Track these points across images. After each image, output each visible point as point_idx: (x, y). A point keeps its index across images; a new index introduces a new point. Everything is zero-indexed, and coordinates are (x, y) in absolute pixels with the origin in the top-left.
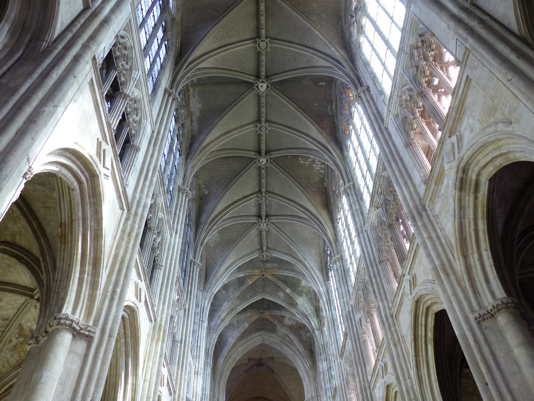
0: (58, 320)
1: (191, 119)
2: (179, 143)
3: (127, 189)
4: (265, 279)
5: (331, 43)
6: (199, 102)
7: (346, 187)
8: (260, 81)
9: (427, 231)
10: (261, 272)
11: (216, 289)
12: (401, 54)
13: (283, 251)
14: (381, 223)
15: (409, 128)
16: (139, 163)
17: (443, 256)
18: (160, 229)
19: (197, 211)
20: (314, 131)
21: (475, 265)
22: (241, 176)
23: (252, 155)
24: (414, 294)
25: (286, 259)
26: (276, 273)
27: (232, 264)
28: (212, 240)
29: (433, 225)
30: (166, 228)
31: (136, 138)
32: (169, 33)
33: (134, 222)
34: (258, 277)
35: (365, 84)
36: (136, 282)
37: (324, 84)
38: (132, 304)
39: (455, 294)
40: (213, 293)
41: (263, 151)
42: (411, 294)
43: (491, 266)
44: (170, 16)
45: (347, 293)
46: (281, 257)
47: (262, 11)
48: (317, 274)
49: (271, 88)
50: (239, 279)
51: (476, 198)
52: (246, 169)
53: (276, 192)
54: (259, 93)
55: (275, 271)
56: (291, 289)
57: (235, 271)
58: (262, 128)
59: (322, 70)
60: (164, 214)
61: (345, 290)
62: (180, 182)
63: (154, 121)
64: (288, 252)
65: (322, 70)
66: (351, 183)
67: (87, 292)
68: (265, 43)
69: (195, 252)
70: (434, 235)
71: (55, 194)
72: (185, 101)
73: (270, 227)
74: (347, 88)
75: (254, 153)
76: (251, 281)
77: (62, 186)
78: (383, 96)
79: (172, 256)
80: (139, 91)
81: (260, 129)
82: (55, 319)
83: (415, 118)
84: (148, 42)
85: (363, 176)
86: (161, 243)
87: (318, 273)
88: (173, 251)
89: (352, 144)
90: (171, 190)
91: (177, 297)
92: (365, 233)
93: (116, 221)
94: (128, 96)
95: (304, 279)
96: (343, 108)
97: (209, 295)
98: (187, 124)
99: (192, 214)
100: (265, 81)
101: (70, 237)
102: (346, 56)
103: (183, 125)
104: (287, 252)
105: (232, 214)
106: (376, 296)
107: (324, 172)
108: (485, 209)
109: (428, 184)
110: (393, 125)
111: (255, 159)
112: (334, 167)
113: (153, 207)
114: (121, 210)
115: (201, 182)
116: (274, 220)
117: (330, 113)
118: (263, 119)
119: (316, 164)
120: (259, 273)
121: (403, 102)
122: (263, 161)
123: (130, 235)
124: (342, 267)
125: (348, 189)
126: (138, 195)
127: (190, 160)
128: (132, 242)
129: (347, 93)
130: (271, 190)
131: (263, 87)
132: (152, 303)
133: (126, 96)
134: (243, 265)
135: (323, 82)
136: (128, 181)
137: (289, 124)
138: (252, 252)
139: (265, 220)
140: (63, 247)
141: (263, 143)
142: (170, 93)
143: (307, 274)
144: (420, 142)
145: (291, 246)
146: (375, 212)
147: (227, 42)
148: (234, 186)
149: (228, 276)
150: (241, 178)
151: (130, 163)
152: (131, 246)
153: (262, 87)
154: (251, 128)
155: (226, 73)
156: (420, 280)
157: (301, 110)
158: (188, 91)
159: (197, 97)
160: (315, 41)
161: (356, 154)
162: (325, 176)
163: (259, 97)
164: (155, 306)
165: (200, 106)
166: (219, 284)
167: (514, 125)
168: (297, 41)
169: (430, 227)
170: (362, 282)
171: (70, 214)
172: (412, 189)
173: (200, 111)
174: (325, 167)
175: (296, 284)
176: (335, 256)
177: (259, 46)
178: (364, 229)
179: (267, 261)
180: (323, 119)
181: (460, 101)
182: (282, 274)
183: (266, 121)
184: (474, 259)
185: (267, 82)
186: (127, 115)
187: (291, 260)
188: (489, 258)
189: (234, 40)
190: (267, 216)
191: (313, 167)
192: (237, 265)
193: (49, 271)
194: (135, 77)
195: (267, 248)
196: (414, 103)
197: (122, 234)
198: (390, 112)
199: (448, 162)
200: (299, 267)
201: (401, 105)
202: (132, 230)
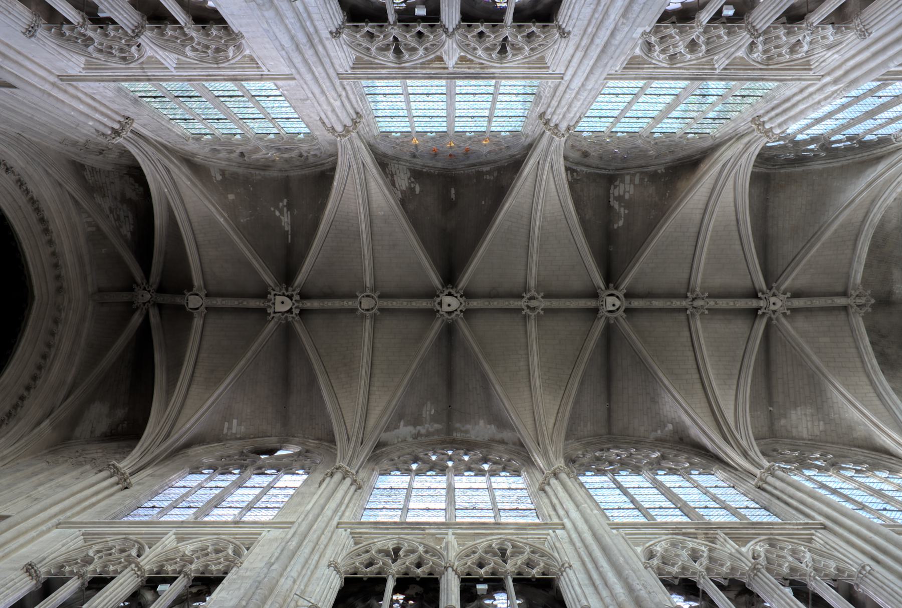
37: (453, 191)
53: (686, 276)
54: (461, 311)
68: (362, 301)
73: (783, 288)
81: (533, 309)
100: (438, 300)
107: (638, 175)
111: (607, 319)
117: (496, 174)
119: (625, 192)
135: (449, 192)
153: (449, 305)
159: (469, 427)
165: (482, 422)
174: (628, 174)
185: (441, 295)
195: (845, 294)
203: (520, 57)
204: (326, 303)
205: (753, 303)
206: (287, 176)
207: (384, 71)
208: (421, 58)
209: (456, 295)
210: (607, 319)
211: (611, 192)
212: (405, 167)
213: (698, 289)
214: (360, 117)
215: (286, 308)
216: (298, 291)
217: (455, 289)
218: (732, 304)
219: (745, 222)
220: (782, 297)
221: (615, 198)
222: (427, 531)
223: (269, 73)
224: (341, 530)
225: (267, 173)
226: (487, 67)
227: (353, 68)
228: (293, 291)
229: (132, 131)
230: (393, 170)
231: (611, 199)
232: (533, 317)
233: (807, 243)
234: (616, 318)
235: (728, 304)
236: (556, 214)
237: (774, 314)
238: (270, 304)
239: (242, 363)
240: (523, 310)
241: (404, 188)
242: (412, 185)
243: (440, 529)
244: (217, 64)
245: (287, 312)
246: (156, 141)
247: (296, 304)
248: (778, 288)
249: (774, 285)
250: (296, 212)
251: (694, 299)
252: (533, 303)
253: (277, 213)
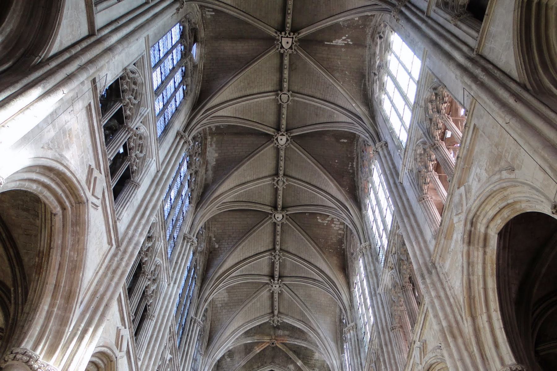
0: (14, 355)
1: (206, 167)
2: (189, 190)
3: (118, 224)
4: (275, 348)
5: (352, 99)
6: (215, 151)
7: (361, 247)
8: (280, 134)
9: (436, 290)
11: (219, 355)
12: (417, 107)
14: (395, 286)
15: (423, 182)
16: (137, 199)
17: (451, 317)
18: (156, 276)
19: (204, 265)
20: (333, 188)
21: (484, 327)
22: (254, 231)
23: (268, 209)
24: (424, 364)
25: (298, 327)
26: (287, 342)
27: (239, 327)
28: (220, 299)
29: (442, 284)
30: (164, 276)
31: (138, 175)
32: (189, 79)
33: (122, 259)
34: (268, 345)
35: (383, 140)
36: (118, 328)
37: (345, 141)
38: (109, 352)
39: (462, 359)
40: (215, 359)
41: (279, 206)
42: (421, 364)
43: (501, 328)
44: (192, 63)
45: (360, 366)
46: (293, 324)
47: (286, 65)
48: (331, 345)
49: (291, 141)
50: (246, 345)
51: (485, 253)
52: (260, 224)
53: (291, 251)
54: (278, 146)
55: (286, 339)
56: (302, 361)
57: (241, 335)
58: (279, 182)
59: (342, 125)
60: (163, 260)
61: (358, 363)
62: (186, 229)
63: (161, 162)
64: (301, 319)
65: (342, 125)
66: (367, 243)
67: (54, 328)
69: (198, 308)
70: (442, 294)
71: (38, 222)
72: (201, 149)
73: (283, 289)
74: (368, 145)
75: (270, 208)
76: (259, 349)
77: (45, 212)
78: (399, 151)
79: (167, 307)
80: (146, 129)
81: (277, 182)
82: (12, 353)
83: (428, 171)
84: (162, 82)
85: (379, 234)
86: (156, 292)
87: (333, 344)
88: (169, 302)
89: (371, 201)
90: (176, 237)
91: (170, 356)
92: (378, 296)
93: (101, 256)
94: (132, 130)
95: (317, 350)
96: (363, 166)
97: (210, 360)
98: (201, 173)
99: (198, 268)
100: (285, 134)
101: (45, 266)
102: (367, 112)
103: (196, 172)
104: (300, 319)
105: (242, 271)
106: (386, 367)
107: (343, 233)
108: (495, 266)
109: (438, 238)
110: (408, 180)
111: (271, 214)
112: (351, 226)
113: (150, 251)
114: (109, 245)
115: (212, 235)
116: (287, 281)
117: (351, 171)
118: (281, 173)
119: (335, 224)
120: (268, 341)
121: (418, 156)
122: (279, 216)
123: (114, 272)
124: (356, 336)
125: (364, 249)
126: (130, 232)
127: (201, 208)
128: (116, 280)
129: (368, 150)
130: (286, 249)
131: (282, 140)
132: (136, 356)
133: (129, 130)
134: (251, 329)
135: (345, 139)
136: (121, 216)
137: (308, 180)
138: (262, 316)
139: (278, 281)
140: (37, 277)
141: (279, 197)
142: (182, 136)
143: (320, 344)
144: (434, 197)
145: (304, 312)
146: (389, 274)
147: (248, 92)
148: (246, 241)
149: (233, 341)
150: (255, 233)
151: (126, 199)
152: (113, 284)
153: (281, 139)
154: (268, 181)
155: (244, 123)
156: (430, 347)
157: (320, 166)
158: (206, 139)
159: (214, 146)
160: (337, 97)
161: (374, 212)
162: (344, 237)
163: (278, 150)
164: (140, 359)
165: (216, 155)
166: (222, 349)
167: (516, 171)
168: (318, 95)
169: (438, 285)
170: (375, 353)
171: (49, 241)
172: (422, 245)
173: (217, 161)
174: (344, 227)
175: (308, 357)
176: (349, 324)
177: (280, 98)
178: (377, 292)
179: (278, 327)
180: (343, 176)
181: (468, 150)
182: (294, 343)
183: (285, 175)
184: (482, 321)
186: (130, 149)
188: (498, 320)
189: (256, 91)
190: (280, 277)
191: (332, 227)
192: (244, 329)
193: (18, 304)
194: (143, 113)
195: (279, 312)
196: (427, 157)
197: (106, 270)
198: (405, 166)
199: (457, 215)
200: (312, 335)
201: (415, 159)
202: (117, 267)
206: (366, 47)
215: (284, 44)
238: (287, 34)
245: (282, 45)
250: (343, 50)
253: (344, 38)
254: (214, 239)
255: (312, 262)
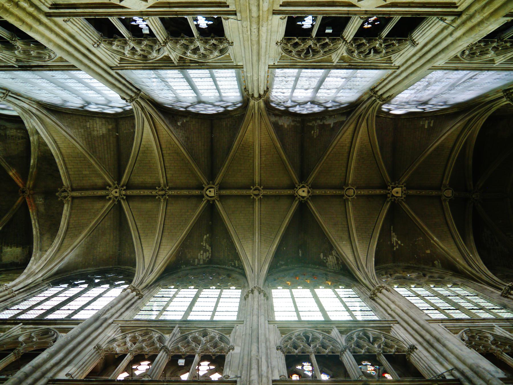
10: (29, 188)
13: (72, 219)
28: (95, 126)
34: (20, 185)
37: (300, 255)
53: (169, 208)
54: (297, 188)
68: (353, 194)
73: (111, 201)
76: (13, 174)
100: (310, 194)
104: (70, 224)
111: (214, 184)
117: (278, 264)
119: (203, 254)
120: (27, 186)
131: (303, 193)
135: (303, 254)
159: (292, 124)
162: (192, 265)
165: (286, 126)
173: (282, 126)
174: (201, 265)
185: (308, 197)
187: (62, 231)
191: (200, 251)
195: (73, 198)
203: (296, 334)
204: (373, 193)
205: (129, 192)
207: (372, 325)
208: (354, 333)
209: (300, 197)
210: (214, 184)
211: (210, 255)
212: (330, 268)
213: (162, 200)
214: (371, 298)
216: (388, 199)
217: (300, 200)
218: (142, 192)
219: (136, 238)
220: (111, 196)
221: (208, 251)
222: (348, 64)
223: (439, 324)
224: (397, 65)
225: (406, 265)
226: (313, 327)
227: (391, 327)
228: (391, 199)
229: (501, 289)
230: (337, 267)
231: (210, 250)
232: (257, 185)
233: (97, 226)
234: (208, 184)
235: (144, 192)
236: (246, 242)
237: (116, 187)
239: (422, 159)
240: (262, 189)
241: (330, 257)
242: (325, 258)
243: (340, 66)
244: (470, 329)
245: (394, 188)
246: (481, 283)
247: (389, 192)
248: (114, 201)
249: (116, 203)
250: (389, 243)
251: (164, 195)
252: (256, 192)
253: (399, 242)
254: (185, 121)
255: (164, 234)
